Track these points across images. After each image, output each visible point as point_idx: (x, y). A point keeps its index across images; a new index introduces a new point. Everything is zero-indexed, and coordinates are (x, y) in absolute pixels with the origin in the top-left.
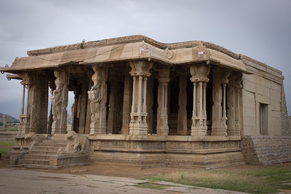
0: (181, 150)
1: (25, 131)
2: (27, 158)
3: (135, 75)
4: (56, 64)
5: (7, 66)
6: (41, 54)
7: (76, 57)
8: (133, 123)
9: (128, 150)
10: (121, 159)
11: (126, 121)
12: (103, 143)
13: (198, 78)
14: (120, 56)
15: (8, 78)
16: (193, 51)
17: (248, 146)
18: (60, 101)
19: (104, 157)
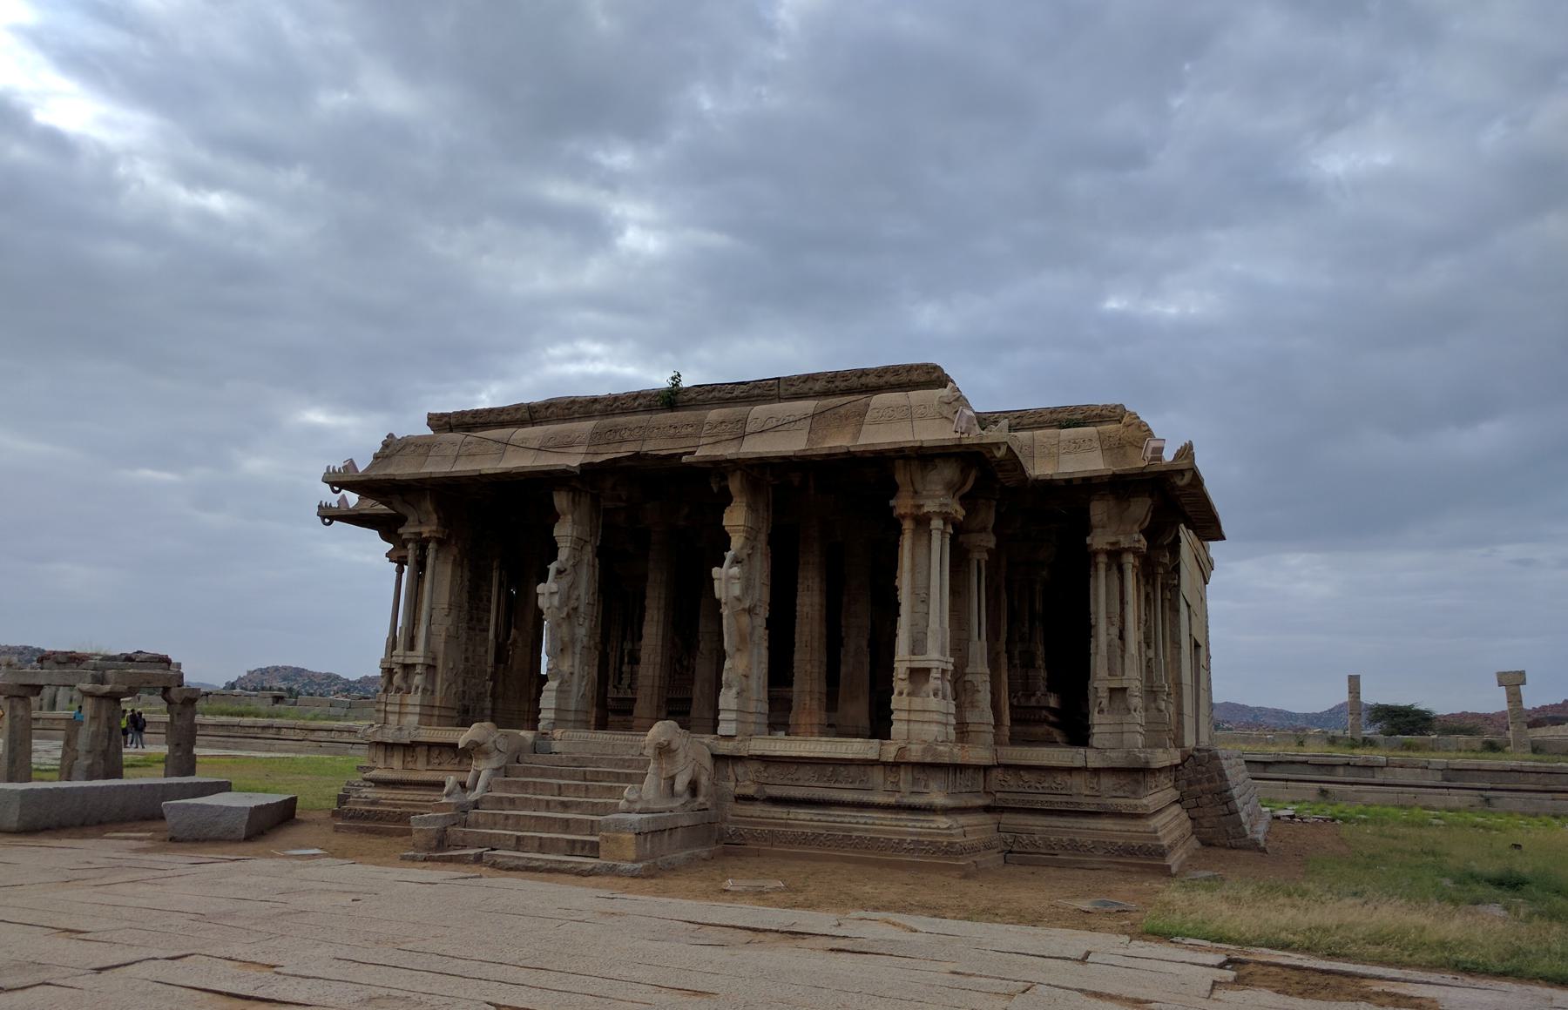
0: (1059, 801)
1: (416, 718)
2: (477, 825)
3: (914, 511)
4: (573, 460)
5: (351, 465)
6: (486, 425)
7: (658, 438)
8: (909, 694)
9: (892, 800)
10: (868, 835)
11: (807, 687)
12: (772, 770)
13: (1122, 538)
14: (856, 436)
15: (323, 518)
16: (1102, 439)
17: (1206, 785)
18: (573, 603)
19: (787, 825)
